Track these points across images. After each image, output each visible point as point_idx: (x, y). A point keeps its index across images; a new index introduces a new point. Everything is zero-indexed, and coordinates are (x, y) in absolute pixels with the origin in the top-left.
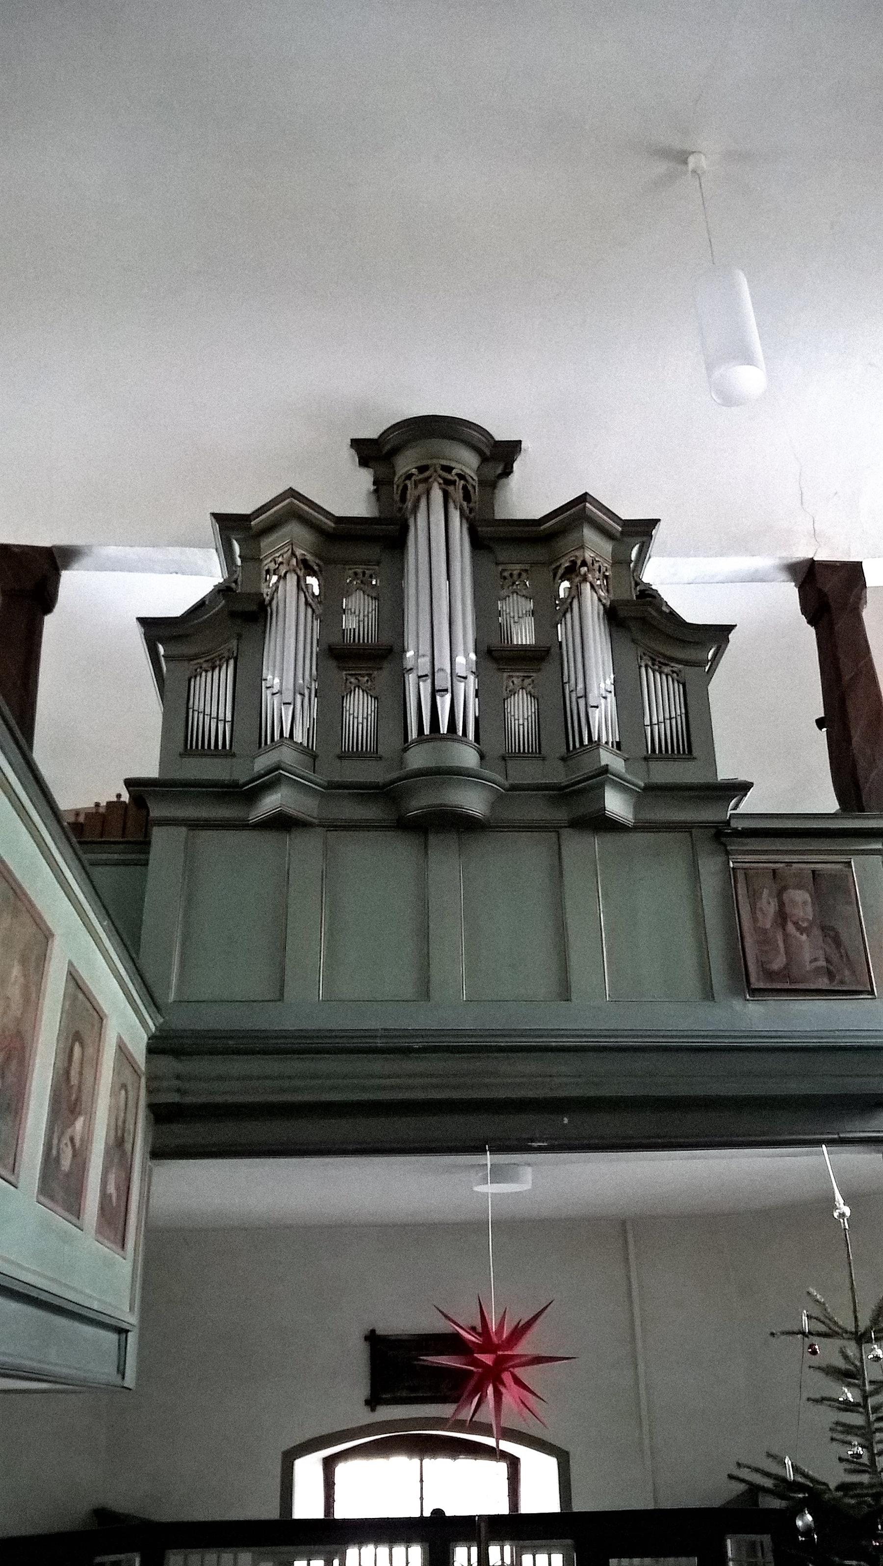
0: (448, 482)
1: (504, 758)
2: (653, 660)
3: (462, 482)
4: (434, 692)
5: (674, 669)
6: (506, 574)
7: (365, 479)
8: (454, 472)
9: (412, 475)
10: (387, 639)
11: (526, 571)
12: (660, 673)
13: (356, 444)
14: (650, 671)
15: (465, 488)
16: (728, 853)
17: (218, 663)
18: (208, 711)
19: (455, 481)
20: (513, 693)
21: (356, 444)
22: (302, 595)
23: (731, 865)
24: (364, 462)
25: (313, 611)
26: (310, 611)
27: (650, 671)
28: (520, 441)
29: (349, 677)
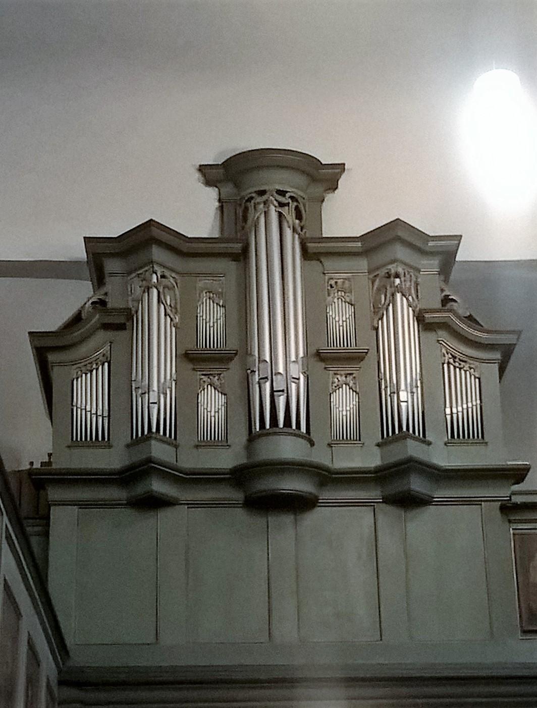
0: (281, 205)
1: (329, 445)
2: (454, 357)
3: (295, 204)
4: (272, 392)
5: (472, 366)
6: (333, 282)
7: (209, 197)
8: (288, 195)
9: (252, 198)
10: (233, 344)
11: (348, 279)
12: (460, 369)
13: (202, 169)
14: (452, 367)
15: (297, 208)
16: (510, 521)
17: (94, 366)
18: (88, 408)
19: (289, 203)
20: (339, 387)
21: (202, 169)
22: (162, 306)
23: (512, 532)
24: (208, 183)
25: (171, 320)
26: (168, 319)
27: (452, 367)
28: (344, 164)
29: (203, 377)
